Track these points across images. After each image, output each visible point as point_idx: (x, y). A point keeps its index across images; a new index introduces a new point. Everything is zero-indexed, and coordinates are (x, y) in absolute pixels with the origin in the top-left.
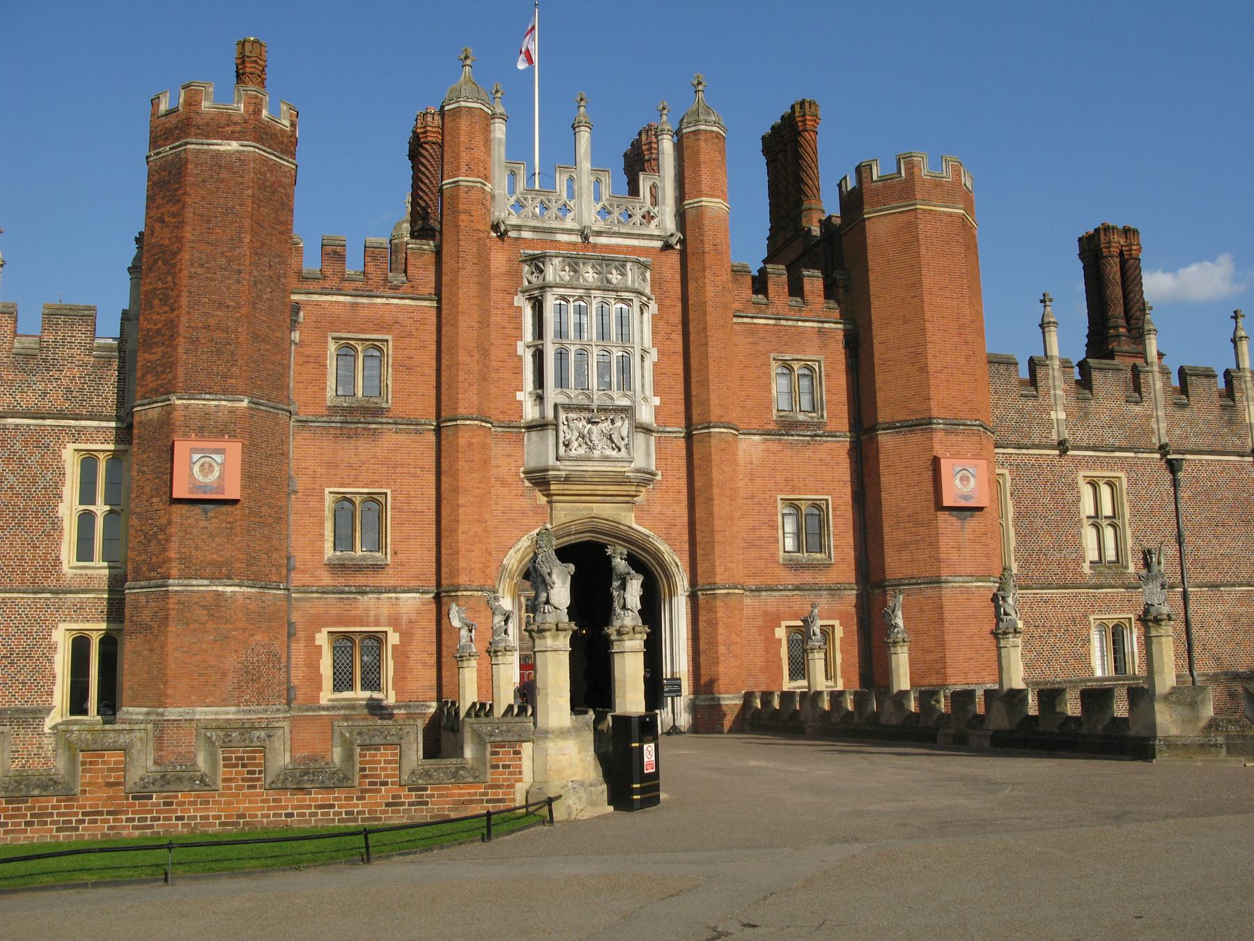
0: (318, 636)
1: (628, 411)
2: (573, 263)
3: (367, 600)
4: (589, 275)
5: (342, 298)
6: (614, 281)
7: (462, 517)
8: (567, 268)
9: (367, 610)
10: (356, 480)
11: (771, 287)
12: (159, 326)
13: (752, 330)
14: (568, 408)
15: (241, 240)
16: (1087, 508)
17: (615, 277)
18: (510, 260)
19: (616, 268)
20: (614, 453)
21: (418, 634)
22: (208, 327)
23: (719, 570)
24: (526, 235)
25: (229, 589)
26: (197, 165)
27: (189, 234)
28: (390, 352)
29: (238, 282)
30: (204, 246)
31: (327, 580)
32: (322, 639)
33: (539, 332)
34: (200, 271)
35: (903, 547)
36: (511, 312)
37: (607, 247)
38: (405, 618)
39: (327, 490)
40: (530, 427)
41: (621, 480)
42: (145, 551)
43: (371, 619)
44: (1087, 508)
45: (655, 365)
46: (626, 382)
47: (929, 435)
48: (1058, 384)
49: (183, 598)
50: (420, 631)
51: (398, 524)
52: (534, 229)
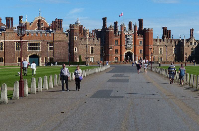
1: (131, 45)
2: (128, 36)
16: (160, 50)
27: (109, 36)
32: (115, 58)
33: (126, 40)
37: (130, 34)
40: (125, 46)
44: (160, 50)
46: (131, 43)
48: (158, 41)
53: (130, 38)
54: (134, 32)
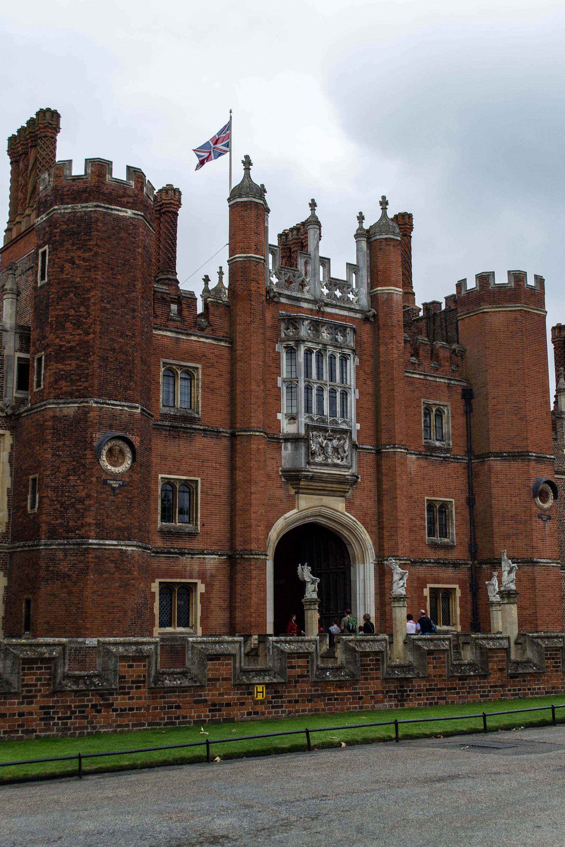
0: (153, 584)
2: (316, 325)
3: (185, 560)
4: (325, 335)
5: (169, 334)
6: (339, 340)
7: (253, 501)
8: (312, 328)
9: (185, 566)
10: (179, 469)
11: (421, 352)
12: (73, 344)
13: (411, 382)
14: (315, 428)
15: (134, 286)
17: (340, 338)
18: (273, 318)
19: (340, 331)
20: (339, 461)
21: (217, 585)
22: (114, 350)
23: (400, 547)
24: (283, 300)
25: (130, 549)
26: (104, 224)
28: (200, 377)
29: (134, 318)
30: (110, 288)
31: (159, 543)
34: (108, 306)
35: (507, 537)
36: (273, 355)
37: (330, 315)
38: (208, 573)
39: (160, 476)
41: (342, 480)
42: (62, 517)
43: (187, 573)
45: (357, 401)
47: (526, 463)
49: (98, 554)
50: (218, 583)
51: (205, 503)
52: (289, 297)
53: (332, 357)
54: (373, 298)
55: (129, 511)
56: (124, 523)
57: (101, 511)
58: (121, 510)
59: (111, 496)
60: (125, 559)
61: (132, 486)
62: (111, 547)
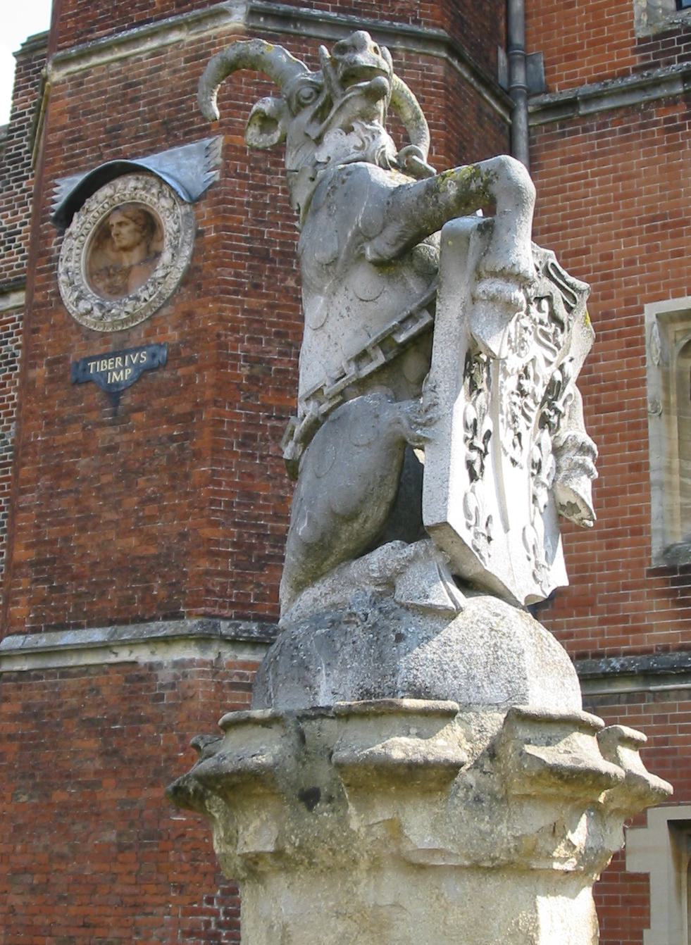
39: (651, 311)
55: (173, 477)
56: (151, 539)
57: (59, 504)
58: (141, 481)
59: (101, 425)
60: (147, 710)
61: (191, 361)
62: (72, 661)
